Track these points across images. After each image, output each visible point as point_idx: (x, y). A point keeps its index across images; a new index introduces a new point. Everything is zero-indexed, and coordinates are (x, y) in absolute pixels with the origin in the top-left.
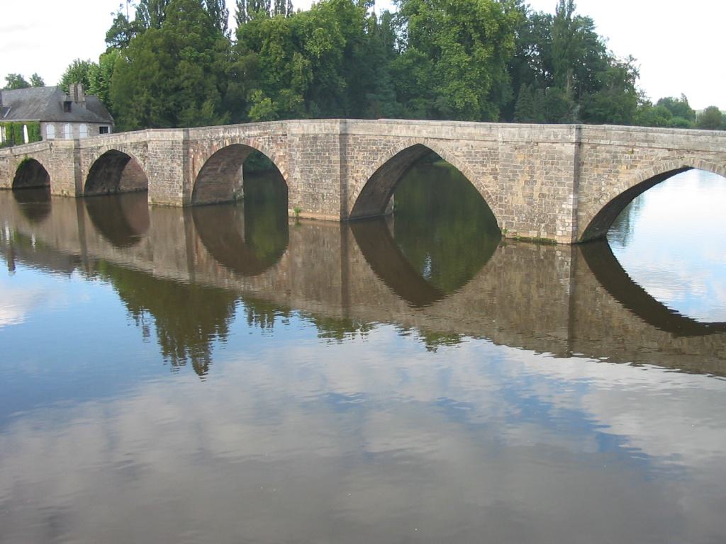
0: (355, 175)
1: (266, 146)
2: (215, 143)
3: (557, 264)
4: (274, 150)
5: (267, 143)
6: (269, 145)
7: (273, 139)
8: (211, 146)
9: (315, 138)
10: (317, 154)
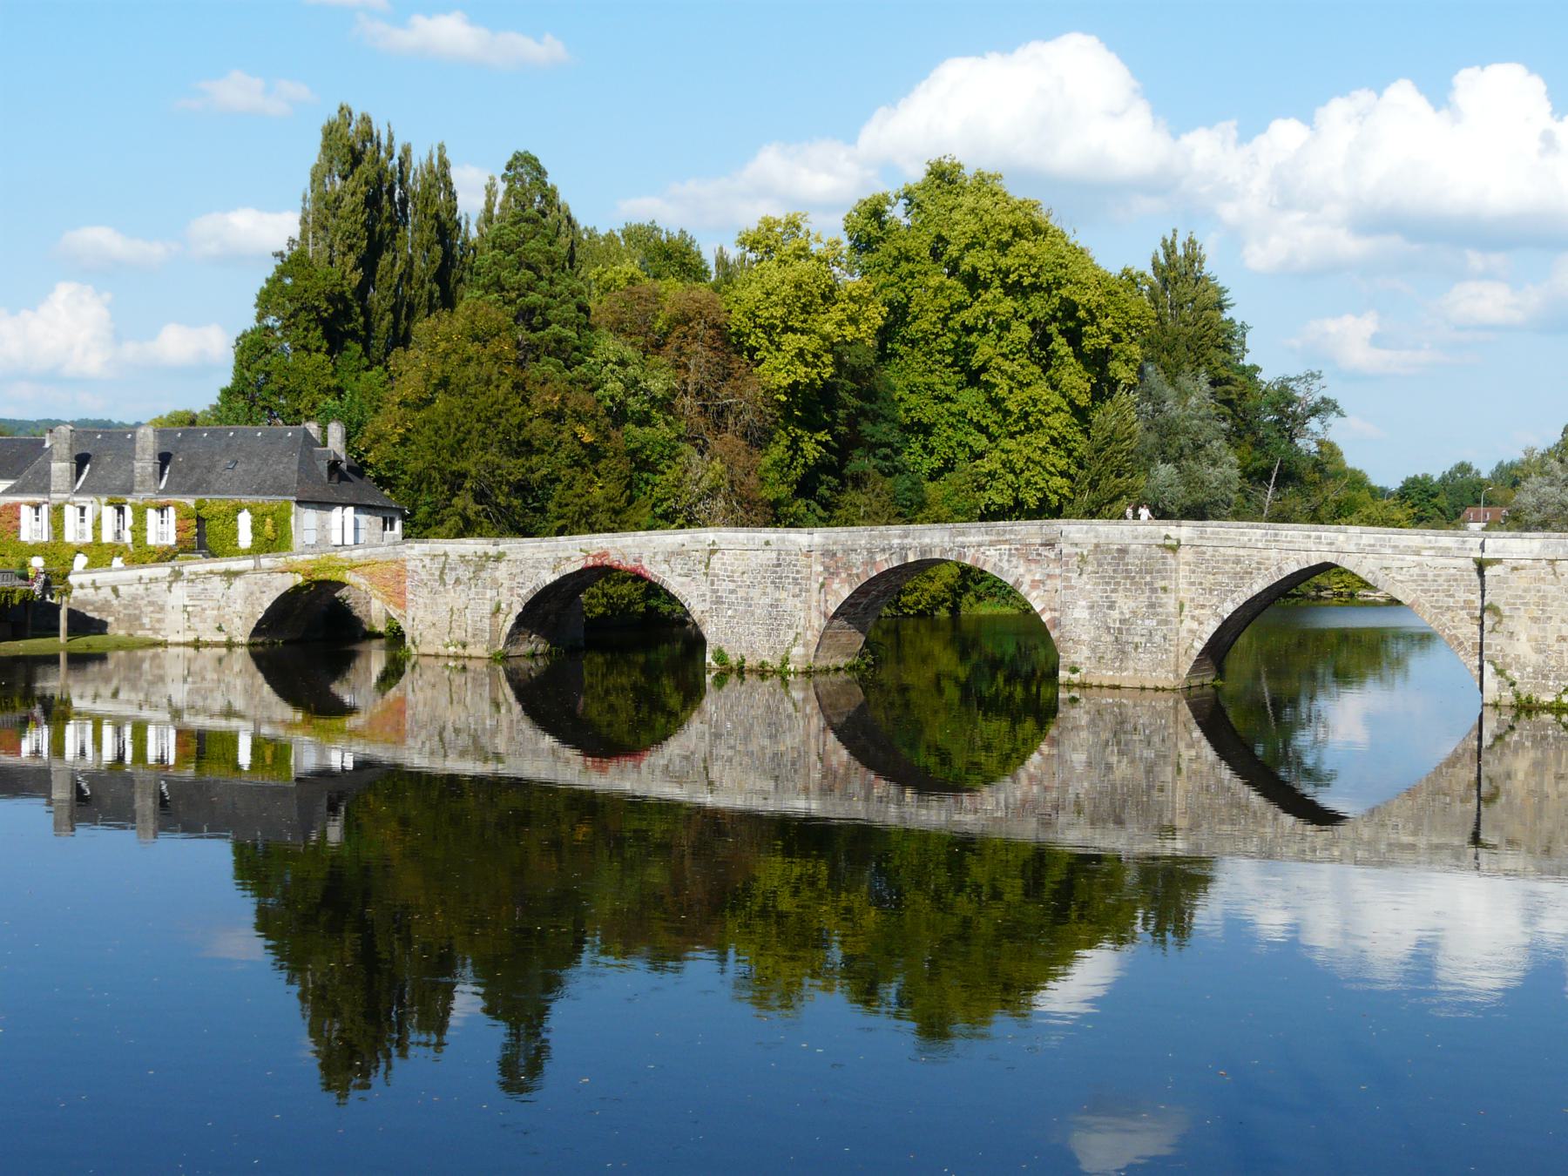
0: (1197, 612)
1: (1005, 565)
2: (879, 558)
4: (1021, 570)
5: (1006, 557)
7: (1026, 554)
8: (871, 562)
9: (1123, 551)
10: (1126, 578)
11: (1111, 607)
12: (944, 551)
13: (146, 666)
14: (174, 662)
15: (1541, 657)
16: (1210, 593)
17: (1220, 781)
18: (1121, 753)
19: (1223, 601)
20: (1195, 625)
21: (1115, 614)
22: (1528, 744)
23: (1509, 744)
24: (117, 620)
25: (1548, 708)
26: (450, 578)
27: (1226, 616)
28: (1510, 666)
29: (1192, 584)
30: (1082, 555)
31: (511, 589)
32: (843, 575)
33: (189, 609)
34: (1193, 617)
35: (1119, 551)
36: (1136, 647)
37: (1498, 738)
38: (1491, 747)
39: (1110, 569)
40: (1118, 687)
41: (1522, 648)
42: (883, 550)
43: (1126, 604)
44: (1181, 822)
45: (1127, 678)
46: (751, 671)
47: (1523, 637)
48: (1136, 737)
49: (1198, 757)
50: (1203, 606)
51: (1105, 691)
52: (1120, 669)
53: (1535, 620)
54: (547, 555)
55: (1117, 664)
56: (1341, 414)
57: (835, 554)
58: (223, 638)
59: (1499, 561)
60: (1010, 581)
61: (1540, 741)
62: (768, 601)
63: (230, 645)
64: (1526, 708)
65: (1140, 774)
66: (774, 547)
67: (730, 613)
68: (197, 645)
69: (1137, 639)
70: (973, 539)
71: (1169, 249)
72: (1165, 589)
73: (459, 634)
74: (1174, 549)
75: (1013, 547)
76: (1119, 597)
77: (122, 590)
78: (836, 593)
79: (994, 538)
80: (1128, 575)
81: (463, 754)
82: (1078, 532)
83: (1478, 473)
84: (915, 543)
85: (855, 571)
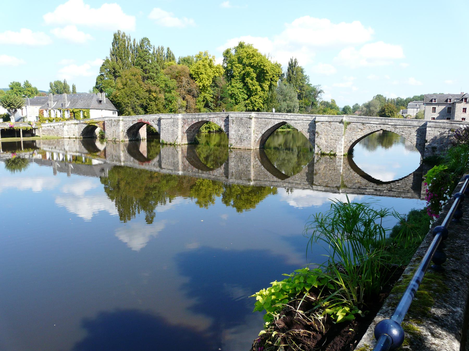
1: (219, 122)
2: (194, 120)
3: (337, 162)
5: (218, 120)
8: (192, 121)
9: (241, 119)
10: (242, 125)
11: (239, 131)
12: (206, 119)
13: (61, 142)
14: (66, 141)
15: (327, 144)
16: (260, 128)
18: (241, 163)
20: (257, 136)
21: (240, 133)
23: (320, 163)
24: (55, 133)
25: (328, 155)
26: (113, 124)
28: (320, 145)
29: (256, 126)
31: (125, 127)
32: (187, 124)
33: (68, 131)
34: (256, 134)
35: (241, 119)
36: (244, 140)
37: (318, 161)
38: (316, 163)
39: (239, 124)
40: (240, 149)
41: (323, 141)
42: (194, 118)
43: (242, 131)
44: (252, 178)
45: (242, 147)
46: (169, 144)
47: (324, 139)
48: (244, 159)
49: (257, 164)
50: (258, 131)
53: (326, 135)
54: (131, 120)
56: (324, 93)
57: (185, 120)
58: (75, 137)
59: (319, 122)
61: (326, 162)
62: (172, 129)
63: (76, 138)
64: (323, 154)
66: (173, 118)
67: (165, 132)
68: (69, 138)
69: (244, 138)
70: (212, 116)
71: (292, 60)
73: (115, 136)
77: (55, 127)
78: (186, 128)
79: (216, 116)
81: (116, 161)
84: (201, 117)
85: (189, 123)
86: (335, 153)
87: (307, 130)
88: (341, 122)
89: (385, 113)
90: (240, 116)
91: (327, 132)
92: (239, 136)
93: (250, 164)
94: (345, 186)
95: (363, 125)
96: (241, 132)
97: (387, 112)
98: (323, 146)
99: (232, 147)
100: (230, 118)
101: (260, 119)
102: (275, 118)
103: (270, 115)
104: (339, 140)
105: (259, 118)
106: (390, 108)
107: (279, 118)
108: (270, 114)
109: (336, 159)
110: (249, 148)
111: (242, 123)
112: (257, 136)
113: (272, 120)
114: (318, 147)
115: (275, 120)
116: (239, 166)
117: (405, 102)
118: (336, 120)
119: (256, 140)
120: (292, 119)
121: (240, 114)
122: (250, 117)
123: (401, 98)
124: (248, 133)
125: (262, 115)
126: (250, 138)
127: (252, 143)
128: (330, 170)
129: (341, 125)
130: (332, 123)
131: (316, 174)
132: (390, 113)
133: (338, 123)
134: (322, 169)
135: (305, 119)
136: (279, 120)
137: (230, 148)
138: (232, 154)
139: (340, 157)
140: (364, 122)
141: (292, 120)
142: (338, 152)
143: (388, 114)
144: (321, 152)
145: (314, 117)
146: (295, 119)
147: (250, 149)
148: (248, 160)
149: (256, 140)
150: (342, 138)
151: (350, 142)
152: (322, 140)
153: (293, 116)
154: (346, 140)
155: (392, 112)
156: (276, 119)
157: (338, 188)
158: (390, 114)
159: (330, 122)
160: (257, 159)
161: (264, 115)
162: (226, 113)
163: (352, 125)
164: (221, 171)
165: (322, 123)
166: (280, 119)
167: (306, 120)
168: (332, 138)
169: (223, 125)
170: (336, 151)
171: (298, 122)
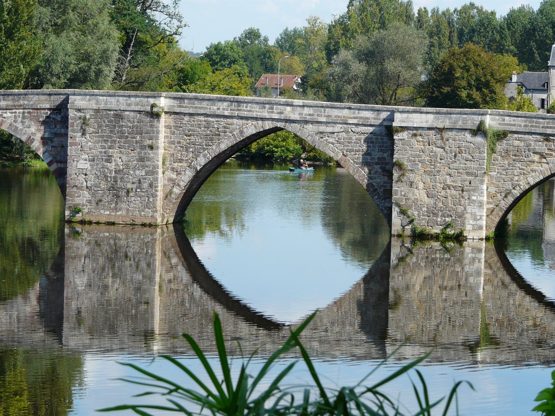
1: (20, 126)
3: (466, 261)
4: (33, 129)
5: (20, 119)
6: (22, 122)
9: (119, 116)
10: (121, 137)
11: (109, 160)
15: (431, 201)
16: (187, 151)
17: (192, 296)
18: (114, 276)
19: (196, 157)
20: (174, 176)
21: (112, 166)
22: (423, 264)
23: (409, 264)
25: (436, 237)
27: (199, 168)
30: (85, 119)
34: (173, 169)
35: (116, 116)
36: (128, 192)
37: (401, 259)
38: (397, 265)
40: (113, 224)
41: (420, 194)
47: (421, 185)
48: (127, 263)
50: (181, 161)
51: (103, 227)
52: (116, 209)
55: (113, 205)
60: (24, 138)
61: (431, 261)
65: (130, 294)
69: (129, 186)
72: (151, 147)
74: (157, 116)
75: (26, 111)
76: (115, 152)
79: (10, 103)
80: (122, 135)
82: (82, 100)
83: (266, 40)
86: (461, 233)
87: (360, 155)
88: (479, 130)
89: (457, 88)
90: (114, 107)
91: (433, 161)
92: (106, 177)
93: (151, 279)
94: (493, 342)
95: (547, 140)
96: (117, 165)
97: (464, 83)
98: (419, 209)
99: (79, 217)
100: (72, 113)
101: (186, 118)
102: (245, 114)
103: (226, 104)
104: (474, 191)
105: (185, 114)
106: (476, 65)
107: (259, 115)
108: (224, 100)
109: (462, 253)
110: (147, 221)
111: (122, 132)
112: (174, 176)
113: (235, 121)
114: (403, 212)
115: (244, 121)
116: (106, 287)
117: (507, 32)
118: (460, 123)
119: (171, 192)
120: (308, 118)
121: (113, 100)
122: (155, 110)
123: (480, 11)
124: (143, 167)
125: (197, 104)
126: (151, 185)
127: (159, 203)
128: (443, 288)
129: (479, 139)
130: (447, 135)
131: (396, 305)
132: (479, 89)
133: (468, 136)
134: (417, 288)
135: (355, 121)
136: (260, 122)
137: (70, 222)
138: (76, 244)
139: (476, 243)
140: (549, 131)
141: (306, 122)
142: (468, 227)
143: (469, 96)
144: (413, 231)
145: (384, 115)
146: (324, 119)
147: (150, 225)
148: (143, 264)
149: (171, 192)
150: (482, 182)
151: (506, 196)
152: (416, 191)
153: (311, 110)
154: (493, 190)
155: (487, 85)
156: (247, 118)
157: (472, 348)
158: (476, 95)
159: (440, 130)
160: (174, 260)
161: (205, 104)
162: (50, 95)
163: (514, 141)
164: (28, 309)
165: (415, 135)
166: (263, 119)
167: (357, 125)
168: (449, 182)
169: (39, 135)
170: (463, 224)
171: (329, 129)
